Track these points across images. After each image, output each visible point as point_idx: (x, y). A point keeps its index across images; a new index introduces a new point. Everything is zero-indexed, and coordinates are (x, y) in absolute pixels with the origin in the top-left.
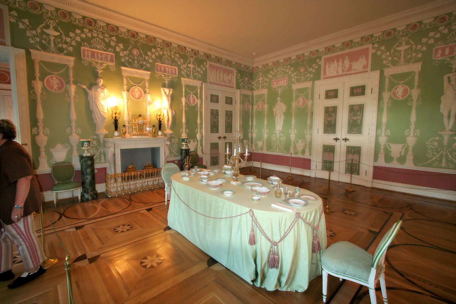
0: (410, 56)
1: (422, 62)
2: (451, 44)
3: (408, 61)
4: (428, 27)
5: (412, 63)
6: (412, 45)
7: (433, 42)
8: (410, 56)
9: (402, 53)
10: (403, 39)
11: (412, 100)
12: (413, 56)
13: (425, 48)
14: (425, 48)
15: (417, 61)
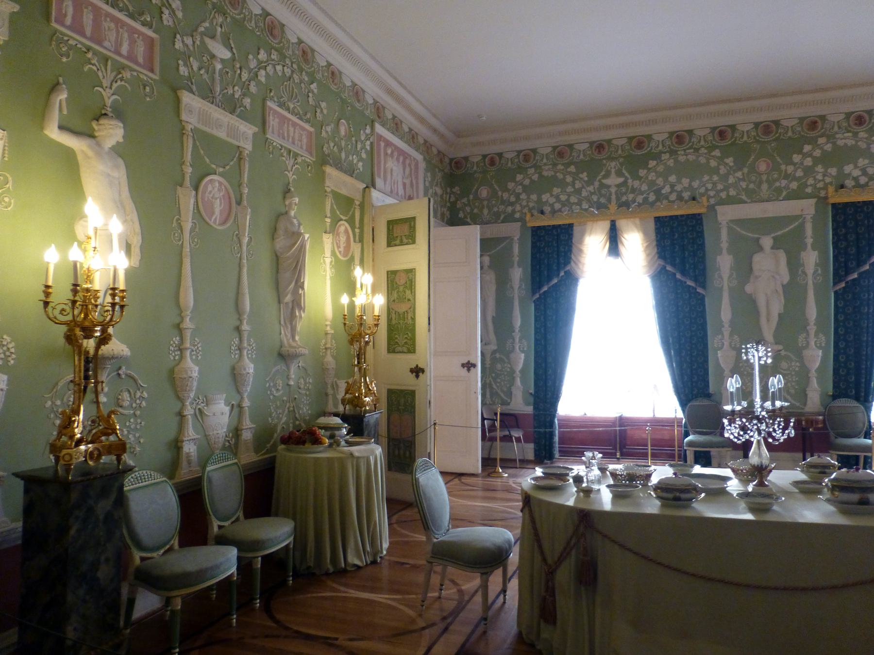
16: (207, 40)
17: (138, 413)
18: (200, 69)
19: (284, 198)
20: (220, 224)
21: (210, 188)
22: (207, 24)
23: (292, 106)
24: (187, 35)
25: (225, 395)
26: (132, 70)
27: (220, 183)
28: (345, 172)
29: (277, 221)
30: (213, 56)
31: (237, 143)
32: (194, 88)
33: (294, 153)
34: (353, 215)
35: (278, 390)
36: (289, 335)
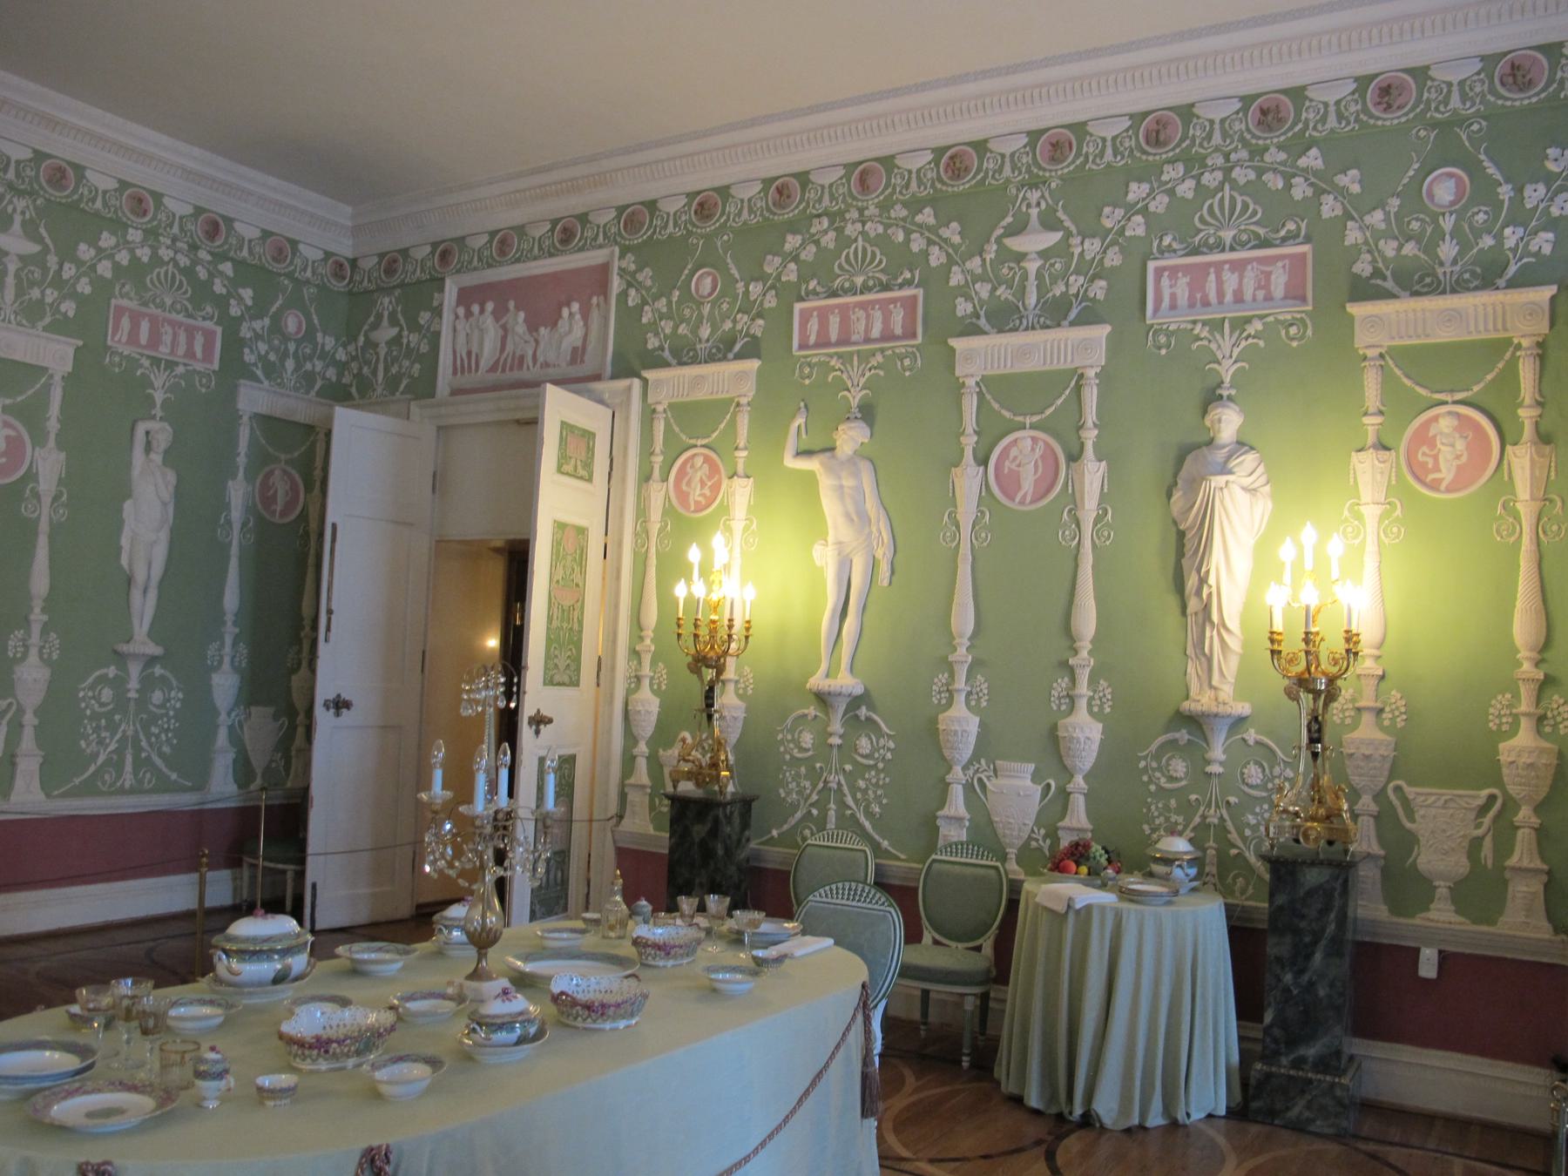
0: (35, 293)
1: (80, 343)
2: (152, 310)
3: (31, 312)
4: (99, 204)
5: (45, 329)
6: (46, 250)
7: (108, 275)
8: (35, 293)
9: (12, 268)
10: (21, 204)
11: (36, 495)
12: (49, 300)
13: (84, 287)
14: (84, 287)
15: (60, 326)
16: (1008, 242)
17: (881, 765)
18: (994, 289)
19: (1205, 412)
20: (1032, 502)
21: (1014, 452)
22: (1009, 219)
23: (1228, 235)
24: (971, 256)
25: (1031, 767)
26: (882, 350)
27: (1034, 439)
28: (1459, 287)
29: (1180, 461)
30: (1021, 257)
31: (1069, 366)
32: (983, 322)
33: (1232, 320)
34: (1509, 377)
35: (1171, 779)
36: (1204, 677)
